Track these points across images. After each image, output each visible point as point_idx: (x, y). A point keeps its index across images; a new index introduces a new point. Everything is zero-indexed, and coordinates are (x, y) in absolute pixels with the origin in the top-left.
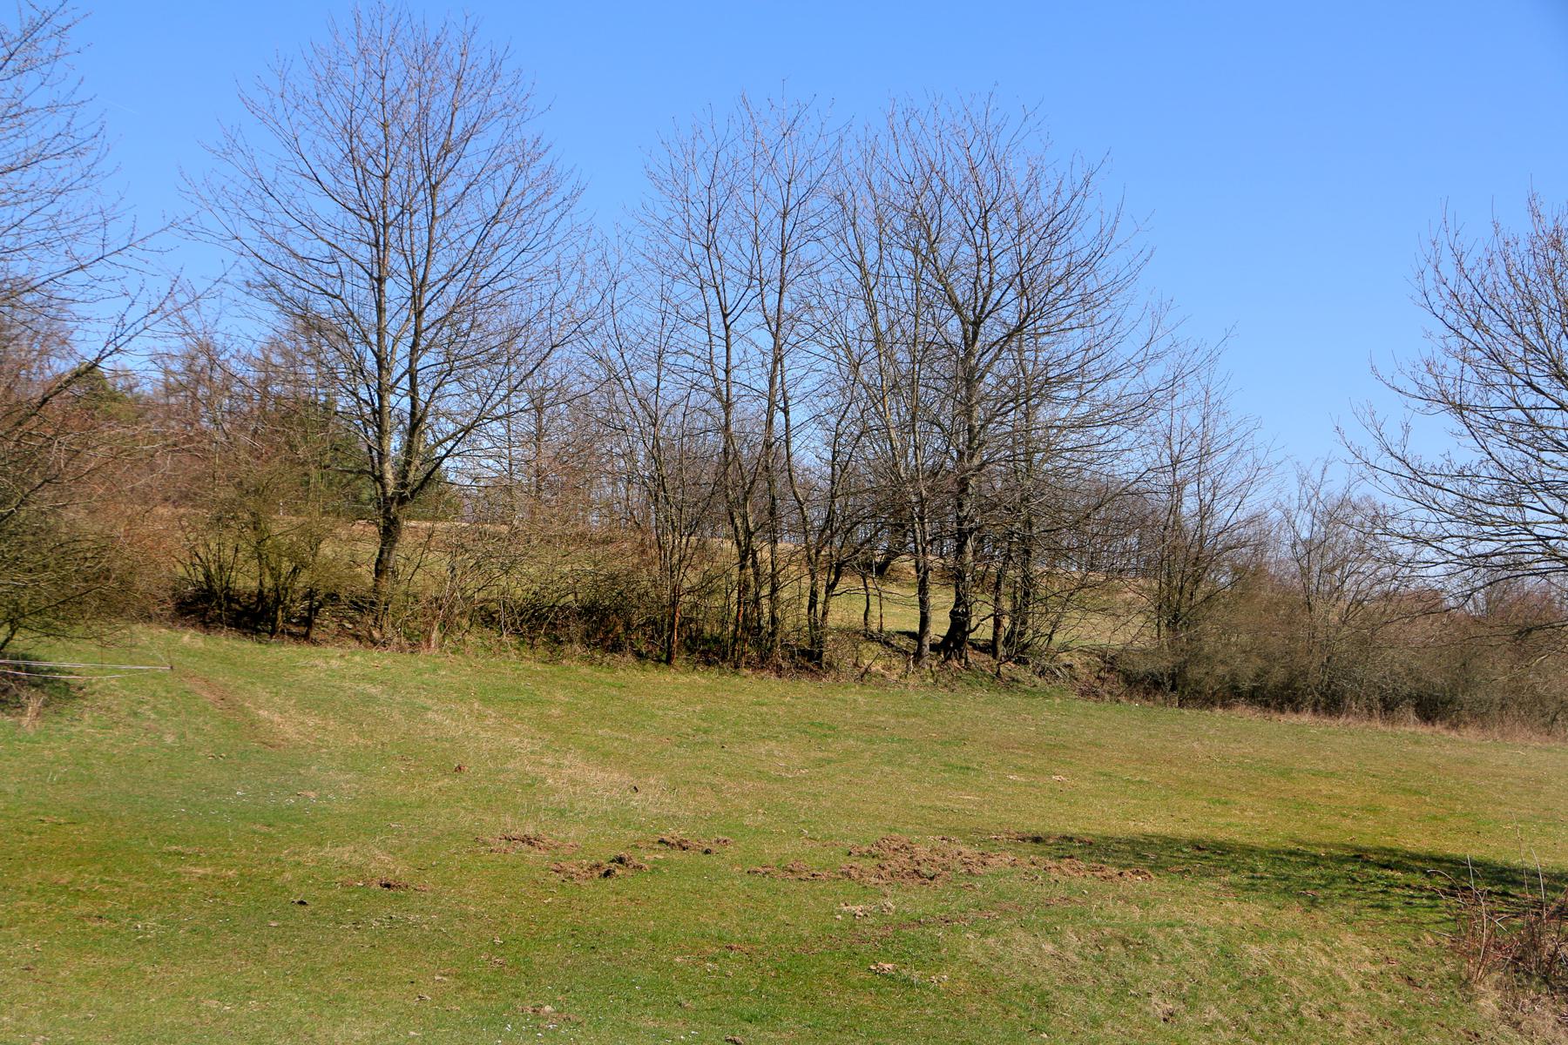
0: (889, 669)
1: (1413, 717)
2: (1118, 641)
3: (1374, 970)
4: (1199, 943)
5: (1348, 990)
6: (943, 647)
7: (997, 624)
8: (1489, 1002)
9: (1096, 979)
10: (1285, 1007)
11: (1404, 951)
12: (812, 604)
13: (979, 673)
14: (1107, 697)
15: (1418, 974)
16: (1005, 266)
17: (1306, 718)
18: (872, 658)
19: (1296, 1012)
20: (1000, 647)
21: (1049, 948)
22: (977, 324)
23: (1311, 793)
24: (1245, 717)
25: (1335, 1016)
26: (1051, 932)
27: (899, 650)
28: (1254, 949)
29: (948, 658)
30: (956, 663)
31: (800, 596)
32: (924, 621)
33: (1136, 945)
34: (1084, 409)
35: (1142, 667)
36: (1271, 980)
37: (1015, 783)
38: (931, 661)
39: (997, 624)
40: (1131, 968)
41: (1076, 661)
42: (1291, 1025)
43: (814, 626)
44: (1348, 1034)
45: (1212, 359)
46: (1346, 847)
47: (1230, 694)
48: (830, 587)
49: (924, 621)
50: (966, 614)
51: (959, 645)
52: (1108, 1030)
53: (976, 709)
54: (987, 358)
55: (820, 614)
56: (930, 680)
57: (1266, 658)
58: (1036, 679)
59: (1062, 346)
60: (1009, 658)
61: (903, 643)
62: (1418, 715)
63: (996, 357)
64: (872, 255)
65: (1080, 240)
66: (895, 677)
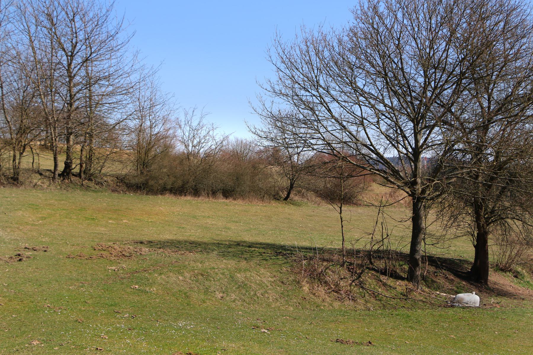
0: (43, 183)
1: (221, 196)
2: (124, 172)
3: (272, 280)
4: (223, 274)
5: (267, 287)
6: (61, 175)
7: (81, 166)
8: (306, 288)
9: (198, 287)
10: (252, 293)
11: (279, 274)
12: (14, 160)
13: (75, 184)
14: (121, 192)
15: (285, 280)
16: (81, 36)
17: (189, 198)
18: (36, 179)
19: (255, 294)
20: (82, 175)
21: (181, 278)
22: (72, 56)
23: (206, 223)
24: (169, 198)
25: (266, 295)
26: (182, 274)
27: (46, 176)
28: (239, 275)
29: (64, 179)
30: (67, 181)
31: (10, 156)
32: (56, 166)
33: (205, 275)
34: (111, 88)
35: (133, 181)
36: (246, 285)
37: (112, 223)
38: (58, 180)
39: (81, 166)
40: (207, 283)
41: (109, 179)
42: (255, 298)
43: (15, 168)
44: (271, 300)
45: (154, 73)
46: (235, 242)
47: (163, 190)
48: (21, 154)
49: (56, 166)
50: (71, 163)
51: (68, 174)
52: (208, 303)
53: (78, 197)
54: (76, 69)
55: (17, 164)
56: (59, 187)
57: (175, 177)
58: (96, 186)
59: (99, 67)
60: (85, 179)
61: (47, 174)
62: (223, 196)
63: (79, 69)
64: (33, 29)
65: (110, 26)
66: (46, 186)
